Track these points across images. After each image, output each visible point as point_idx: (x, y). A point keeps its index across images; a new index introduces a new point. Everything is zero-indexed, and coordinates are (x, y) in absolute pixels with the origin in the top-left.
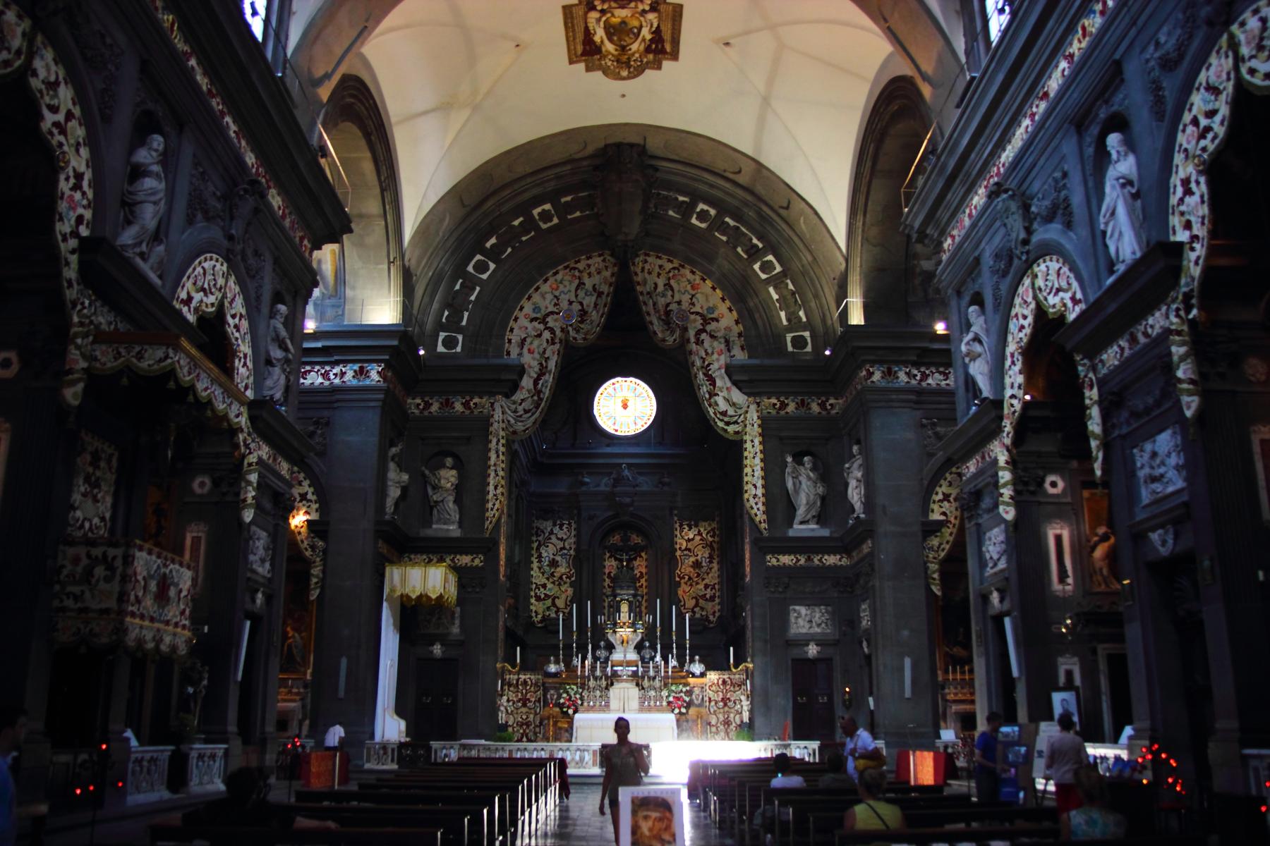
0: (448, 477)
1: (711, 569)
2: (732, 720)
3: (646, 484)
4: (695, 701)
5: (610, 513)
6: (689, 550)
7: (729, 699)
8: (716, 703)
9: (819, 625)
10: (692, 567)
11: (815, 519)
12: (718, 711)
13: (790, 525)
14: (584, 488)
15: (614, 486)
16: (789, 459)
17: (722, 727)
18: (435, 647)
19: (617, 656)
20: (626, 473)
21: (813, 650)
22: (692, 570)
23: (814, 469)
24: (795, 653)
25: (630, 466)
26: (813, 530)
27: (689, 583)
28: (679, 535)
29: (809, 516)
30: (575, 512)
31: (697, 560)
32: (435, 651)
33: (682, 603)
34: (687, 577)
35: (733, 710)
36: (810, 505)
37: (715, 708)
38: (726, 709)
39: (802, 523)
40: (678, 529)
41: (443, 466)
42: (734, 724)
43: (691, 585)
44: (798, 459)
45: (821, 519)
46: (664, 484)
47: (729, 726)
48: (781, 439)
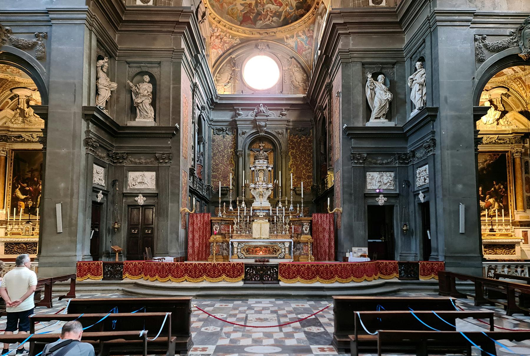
0: (146, 88)
3: (274, 115)
4: (305, 232)
5: (254, 131)
9: (386, 184)
11: (385, 116)
13: (368, 120)
14: (239, 117)
15: (256, 116)
16: (370, 76)
18: (139, 197)
19: (256, 204)
20: (262, 108)
21: (381, 201)
23: (385, 84)
24: (370, 201)
25: (264, 105)
26: (383, 123)
29: (381, 114)
30: (235, 130)
32: (139, 201)
36: (382, 108)
39: (376, 118)
41: (143, 81)
44: (375, 77)
45: (389, 116)
46: (283, 115)
48: (363, 64)
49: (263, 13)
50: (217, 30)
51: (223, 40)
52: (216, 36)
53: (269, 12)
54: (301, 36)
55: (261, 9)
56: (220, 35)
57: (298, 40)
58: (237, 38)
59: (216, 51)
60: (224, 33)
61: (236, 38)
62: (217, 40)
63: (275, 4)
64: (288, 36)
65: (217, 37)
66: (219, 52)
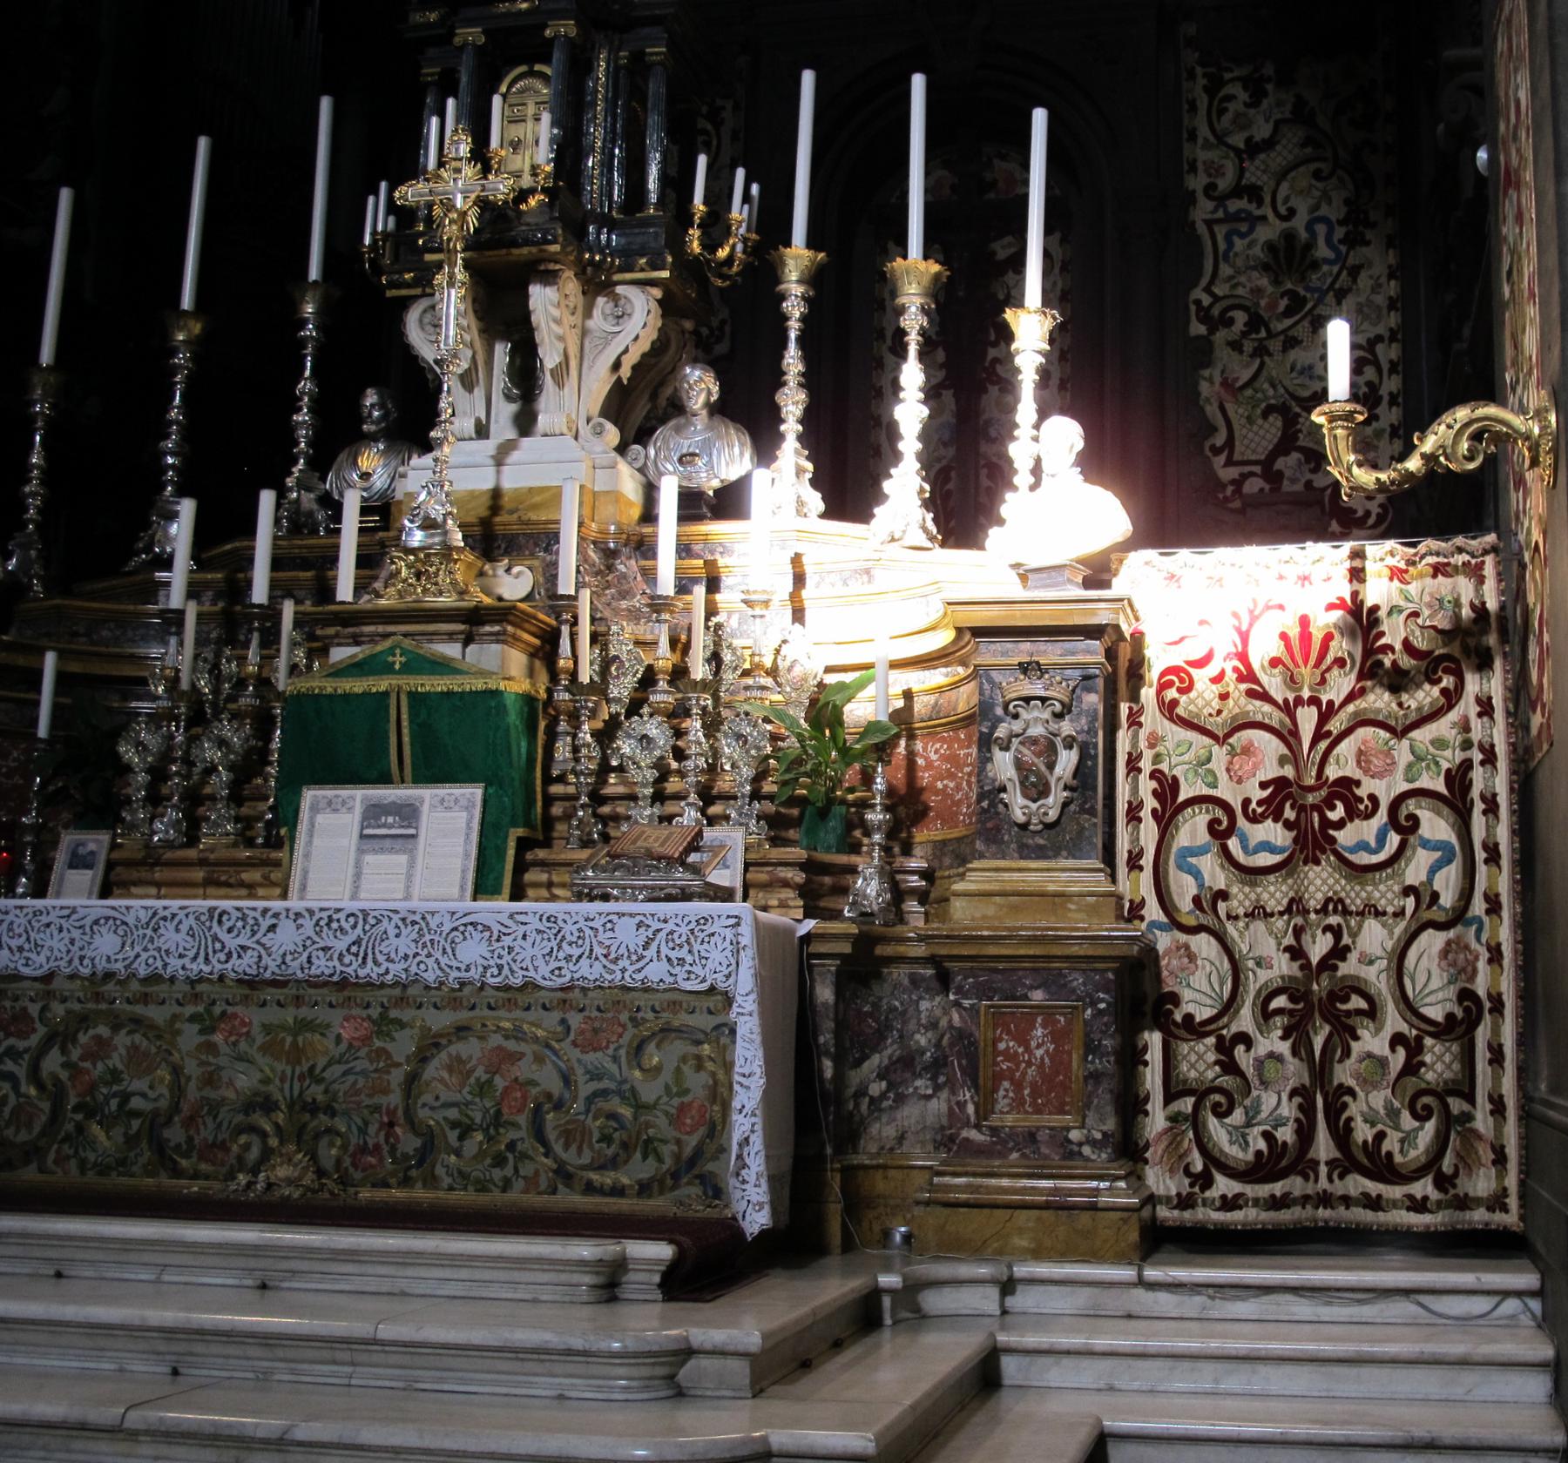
1: (1354, 272)
2: (1376, 977)
4: (1018, 805)
6: (1254, 193)
7: (1346, 785)
8: (1220, 833)
10: (1266, 268)
12: (1241, 897)
17: (1273, 1042)
22: (1264, 282)
27: (1248, 346)
28: (1204, 131)
31: (1289, 236)
33: (1220, 439)
34: (1240, 318)
35: (1384, 893)
37: (1214, 873)
38: (1320, 880)
40: (1203, 102)
42: (1394, 1021)
43: (1261, 351)
47: (1344, 1031)
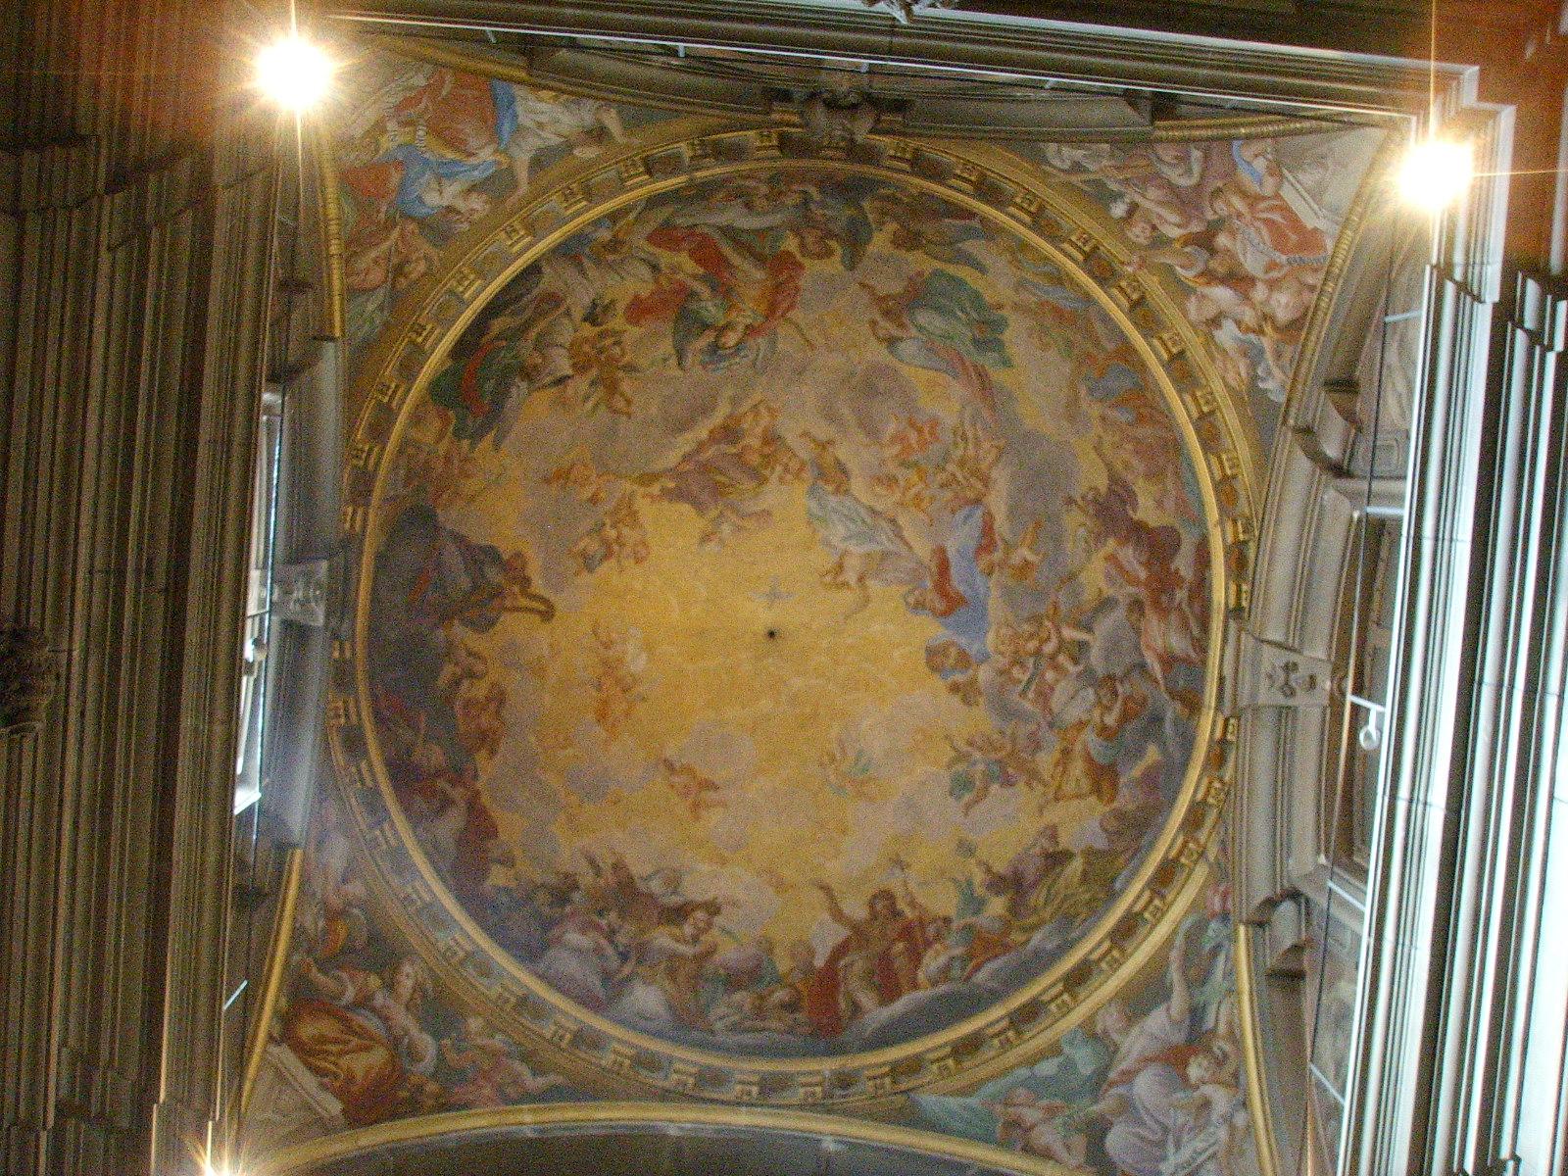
49: (813, 191)
50: (1215, 322)
51: (1196, 227)
52: (1246, 298)
53: (764, 189)
54: (472, 189)
55: (823, 205)
56: (1210, 276)
57: (486, 154)
58: (1063, 177)
59: (1288, 194)
60: (1170, 269)
61: (1075, 179)
62: (1252, 264)
63: (706, 230)
64: (587, 153)
65: (1237, 280)
66: (1260, 164)
